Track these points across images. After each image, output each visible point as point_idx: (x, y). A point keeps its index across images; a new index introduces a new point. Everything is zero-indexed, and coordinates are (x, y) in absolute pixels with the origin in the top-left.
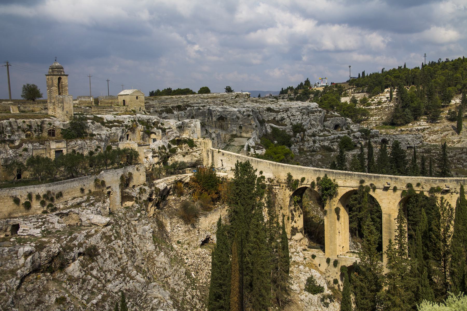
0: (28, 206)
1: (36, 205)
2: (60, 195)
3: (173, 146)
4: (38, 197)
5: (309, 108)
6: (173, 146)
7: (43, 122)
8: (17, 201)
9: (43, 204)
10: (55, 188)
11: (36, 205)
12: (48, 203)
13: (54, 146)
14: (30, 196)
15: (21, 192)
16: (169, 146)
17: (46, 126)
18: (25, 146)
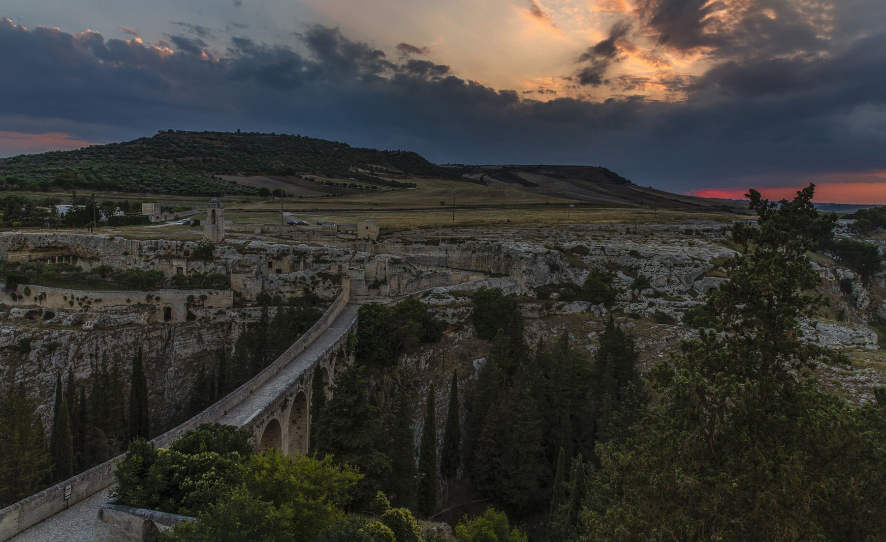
0: (72, 303)
1: (76, 303)
2: (98, 301)
3: (318, 279)
4: (78, 299)
5: (678, 259)
6: (318, 279)
7: (183, 245)
8: (65, 298)
9: (80, 304)
10: (92, 295)
11: (76, 303)
12: (84, 304)
13: (176, 263)
14: (73, 297)
15: (69, 293)
16: (313, 278)
17: (185, 248)
18: (154, 261)
